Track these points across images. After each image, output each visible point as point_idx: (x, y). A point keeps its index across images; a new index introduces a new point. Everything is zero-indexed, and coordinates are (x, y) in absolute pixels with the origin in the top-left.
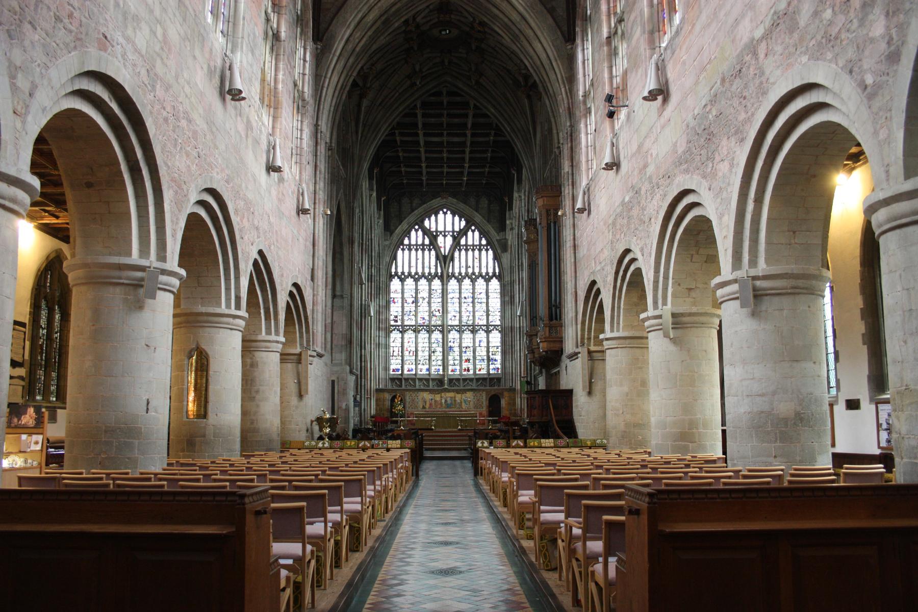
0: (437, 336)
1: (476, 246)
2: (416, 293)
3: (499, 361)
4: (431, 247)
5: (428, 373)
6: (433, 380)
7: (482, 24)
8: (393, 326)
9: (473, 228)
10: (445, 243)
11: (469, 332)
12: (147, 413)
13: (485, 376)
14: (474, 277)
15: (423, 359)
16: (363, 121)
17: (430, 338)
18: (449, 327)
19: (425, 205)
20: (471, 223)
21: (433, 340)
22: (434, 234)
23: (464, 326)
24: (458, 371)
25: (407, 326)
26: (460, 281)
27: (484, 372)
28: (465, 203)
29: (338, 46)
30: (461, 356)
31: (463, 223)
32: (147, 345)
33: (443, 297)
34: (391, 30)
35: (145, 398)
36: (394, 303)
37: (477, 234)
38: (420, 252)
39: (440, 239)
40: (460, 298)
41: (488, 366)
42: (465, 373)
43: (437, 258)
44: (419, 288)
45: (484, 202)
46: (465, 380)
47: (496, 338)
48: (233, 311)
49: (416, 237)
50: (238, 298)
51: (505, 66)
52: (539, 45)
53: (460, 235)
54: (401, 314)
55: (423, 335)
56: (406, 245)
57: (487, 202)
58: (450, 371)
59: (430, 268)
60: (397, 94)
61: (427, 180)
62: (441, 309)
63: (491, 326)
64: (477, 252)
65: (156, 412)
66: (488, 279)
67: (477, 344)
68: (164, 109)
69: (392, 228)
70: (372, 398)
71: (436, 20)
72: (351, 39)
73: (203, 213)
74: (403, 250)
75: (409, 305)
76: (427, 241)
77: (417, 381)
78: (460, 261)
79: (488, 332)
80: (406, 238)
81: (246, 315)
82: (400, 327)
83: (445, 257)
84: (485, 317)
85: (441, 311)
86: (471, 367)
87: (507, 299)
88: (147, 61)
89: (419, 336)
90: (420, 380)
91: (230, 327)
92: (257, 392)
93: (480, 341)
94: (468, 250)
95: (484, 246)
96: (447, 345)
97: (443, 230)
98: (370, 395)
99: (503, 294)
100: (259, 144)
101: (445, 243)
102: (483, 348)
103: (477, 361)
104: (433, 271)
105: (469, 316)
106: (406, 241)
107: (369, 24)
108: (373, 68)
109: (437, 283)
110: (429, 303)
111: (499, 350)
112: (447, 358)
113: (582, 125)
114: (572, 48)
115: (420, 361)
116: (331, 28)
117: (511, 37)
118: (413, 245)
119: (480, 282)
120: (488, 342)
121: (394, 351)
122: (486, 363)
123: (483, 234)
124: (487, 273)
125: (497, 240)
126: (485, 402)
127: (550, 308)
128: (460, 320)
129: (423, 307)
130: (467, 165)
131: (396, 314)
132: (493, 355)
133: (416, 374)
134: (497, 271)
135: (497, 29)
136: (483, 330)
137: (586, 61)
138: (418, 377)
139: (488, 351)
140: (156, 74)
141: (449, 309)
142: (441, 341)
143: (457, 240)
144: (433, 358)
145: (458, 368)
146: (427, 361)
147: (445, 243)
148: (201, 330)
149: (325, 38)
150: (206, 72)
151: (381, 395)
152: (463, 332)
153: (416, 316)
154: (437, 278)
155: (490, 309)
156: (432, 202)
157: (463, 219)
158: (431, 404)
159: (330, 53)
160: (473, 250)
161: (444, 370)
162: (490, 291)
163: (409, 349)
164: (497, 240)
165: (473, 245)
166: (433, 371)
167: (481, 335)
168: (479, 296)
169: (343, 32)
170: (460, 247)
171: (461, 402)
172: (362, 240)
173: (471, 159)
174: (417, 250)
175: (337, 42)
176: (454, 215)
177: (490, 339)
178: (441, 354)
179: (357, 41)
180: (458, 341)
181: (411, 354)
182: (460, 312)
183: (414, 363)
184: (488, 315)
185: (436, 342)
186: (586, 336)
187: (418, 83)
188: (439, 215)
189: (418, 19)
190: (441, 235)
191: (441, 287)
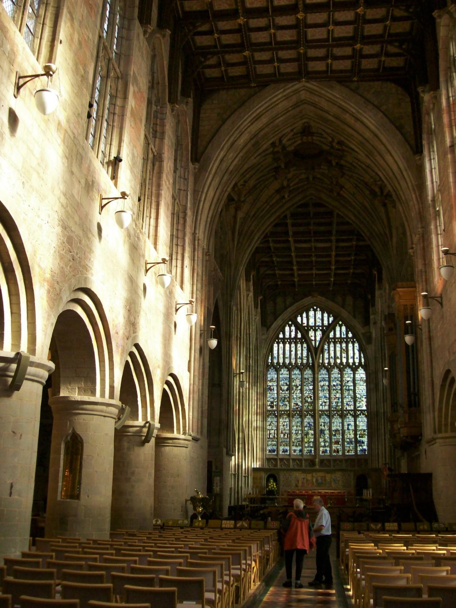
0: (308, 420)
1: (344, 338)
2: (290, 381)
3: (366, 443)
4: (303, 340)
5: (301, 453)
6: (306, 460)
7: (340, 143)
8: (269, 411)
9: (340, 323)
10: (315, 336)
11: (338, 417)
12: (10, 496)
13: (354, 457)
14: (342, 366)
15: (296, 441)
16: (239, 230)
17: (302, 422)
18: (320, 412)
20: (338, 319)
21: (305, 424)
22: (306, 328)
24: (328, 452)
25: (282, 411)
26: (329, 370)
27: (352, 453)
28: (333, 301)
29: (214, 166)
30: (330, 438)
31: (331, 319)
32: (14, 432)
33: (314, 385)
34: (260, 151)
35: (9, 482)
36: (271, 390)
37: (344, 328)
38: (293, 345)
39: (312, 333)
40: (329, 386)
41: (356, 448)
42: (335, 454)
43: (309, 350)
44: (293, 377)
45: (349, 300)
46: (335, 460)
47: (362, 423)
48: (107, 399)
49: (290, 331)
50: (112, 387)
51: (362, 178)
52: (390, 158)
53: (330, 329)
55: (296, 420)
56: (281, 339)
58: (321, 452)
59: (302, 358)
60: (268, 206)
61: (298, 281)
62: (312, 396)
63: (359, 411)
64: (344, 345)
65: (19, 495)
66: (354, 369)
67: (346, 427)
68: (39, 217)
70: (250, 476)
71: (299, 142)
72: (225, 159)
73: (79, 310)
74: (278, 343)
75: (284, 392)
76: (299, 336)
77: (291, 461)
78: (329, 353)
79: (355, 417)
80: (281, 333)
81: (119, 404)
83: (316, 349)
84: (352, 403)
85: (312, 398)
86: (339, 447)
87: (372, 386)
88: (23, 175)
90: (294, 460)
91: (103, 414)
92: (133, 473)
93: (348, 425)
94: (337, 342)
95: (350, 338)
96: (318, 428)
97: (313, 325)
98: (248, 474)
99: (368, 381)
100: (137, 249)
101: (316, 336)
102: (351, 431)
103: (346, 443)
104: (305, 361)
105: (338, 402)
106: (281, 336)
107: (240, 147)
108: (247, 184)
109: (308, 373)
110: (302, 391)
111: (366, 433)
112: (319, 441)
113: (432, 227)
114: (420, 159)
115: (294, 442)
116: (207, 151)
117: (367, 153)
118: (287, 339)
119: (348, 371)
120: (356, 425)
121: (270, 434)
124: (354, 363)
126: (353, 482)
127: (409, 395)
128: (329, 406)
129: (297, 394)
130: (333, 267)
131: (272, 400)
132: (360, 437)
133: (290, 455)
134: (363, 360)
135: (353, 147)
136: (351, 415)
137: (433, 170)
138: (292, 457)
139: (355, 435)
140: (31, 186)
141: (320, 395)
142: (312, 424)
143: (326, 334)
144: (306, 440)
145: (328, 449)
146: (300, 443)
147: (315, 336)
148: (76, 418)
149: (202, 159)
150: (84, 186)
151: (258, 474)
152: (333, 417)
153: (289, 402)
154: (308, 368)
155: (358, 396)
156: (304, 300)
157: (331, 315)
158: (303, 483)
159: (207, 171)
160: (341, 343)
161: (315, 451)
163: (284, 432)
164: (362, 334)
165: (341, 338)
167: (350, 420)
169: (217, 153)
170: (329, 340)
171: (331, 481)
172: (240, 335)
173: (337, 262)
174: (290, 344)
175: (213, 162)
177: (357, 423)
178: (313, 437)
179: (230, 161)
181: (286, 437)
182: (330, 398)
183: (288, 445)
184: (355, 402)
185: (308, 425)
186: (443, 422)
187: (286, 196)
188: (310, 312)
189: (284, 141)
191: (312, 377)
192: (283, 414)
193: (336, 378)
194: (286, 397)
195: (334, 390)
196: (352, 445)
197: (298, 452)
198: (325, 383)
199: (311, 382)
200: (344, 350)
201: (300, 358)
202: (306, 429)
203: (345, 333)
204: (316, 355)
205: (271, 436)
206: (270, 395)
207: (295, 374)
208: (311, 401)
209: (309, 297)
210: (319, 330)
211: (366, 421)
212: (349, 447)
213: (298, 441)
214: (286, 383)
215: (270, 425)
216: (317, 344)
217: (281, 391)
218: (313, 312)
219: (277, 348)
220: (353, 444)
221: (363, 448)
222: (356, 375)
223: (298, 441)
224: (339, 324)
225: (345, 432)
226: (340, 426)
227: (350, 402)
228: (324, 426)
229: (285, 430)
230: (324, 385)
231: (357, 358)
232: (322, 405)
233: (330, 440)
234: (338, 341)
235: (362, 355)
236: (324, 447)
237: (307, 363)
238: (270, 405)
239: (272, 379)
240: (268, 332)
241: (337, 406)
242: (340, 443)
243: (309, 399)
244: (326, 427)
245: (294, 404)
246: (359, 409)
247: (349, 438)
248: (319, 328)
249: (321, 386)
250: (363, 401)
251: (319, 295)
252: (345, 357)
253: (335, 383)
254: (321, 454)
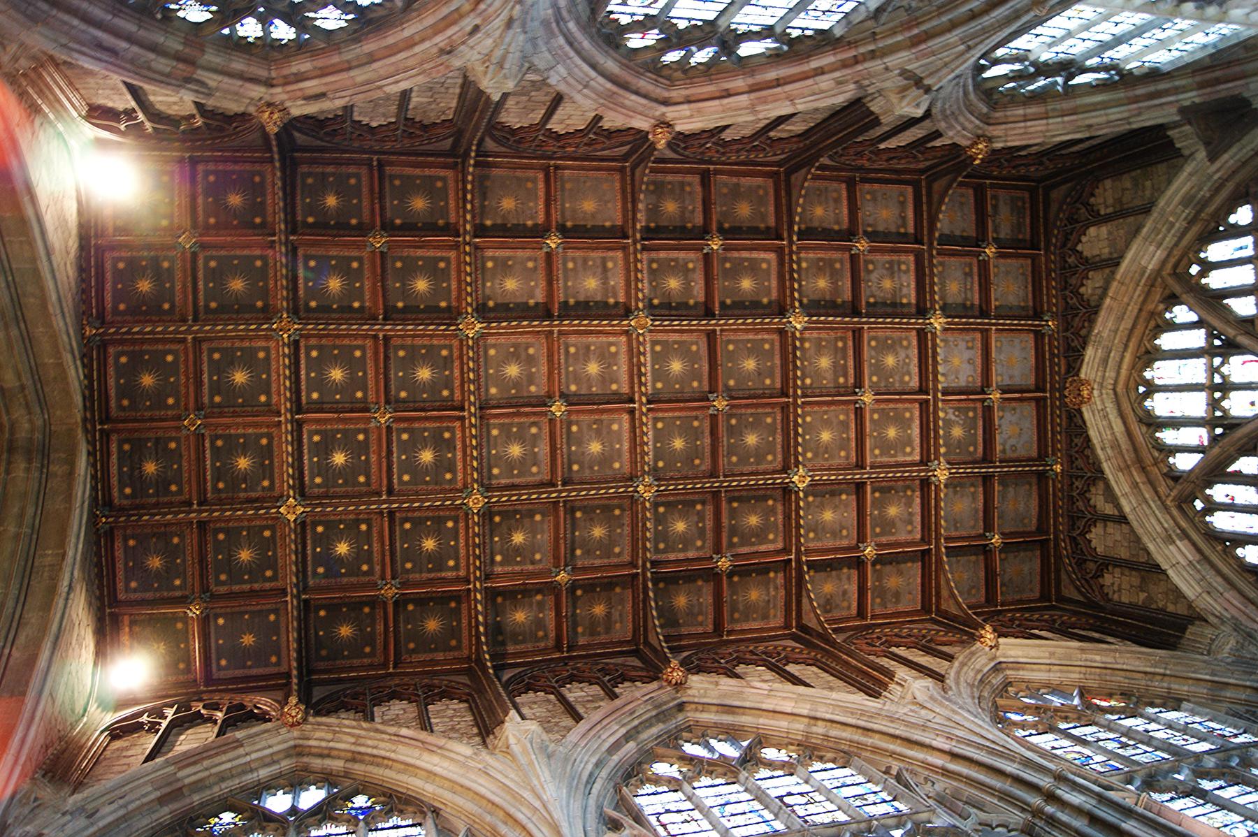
9: (1194, 269)
19: (1106, 467)
28: (1092, 311)
31: (1182, 314)
37: (1216, 251)
45: (1095, 241)
57: (1092, 231)
69: (1181, 610)
80: (1240, 552)
123: (1219, 230)
125: (1212, 158)
157: (1168, 315)
164: (1212, 158)
176: (1153, 355)
188: (1158, 412)
190: (1225, 404)
209: (1087, 415)
210: (1225, 370)
218: (1157, 396)
224: (1203, 274)
240: (1211, 619)
251: (1079, 370)
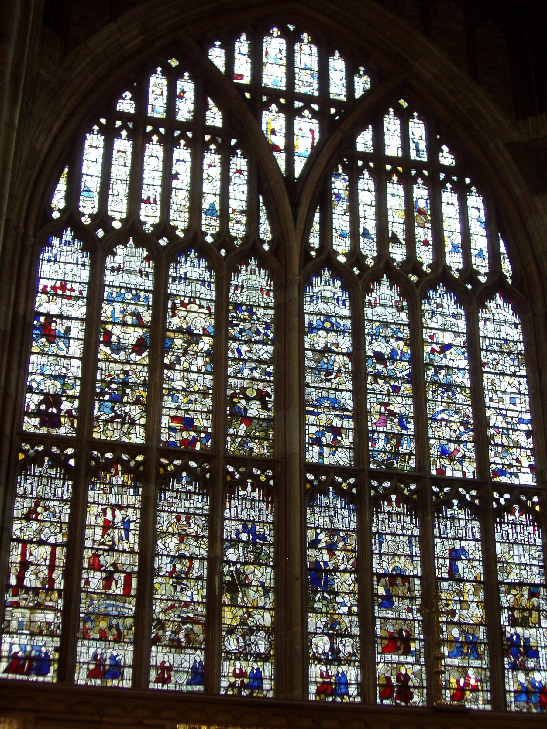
1: (419, 166)
4: (233, 142)
8: (33, 439)
10: (290, 134)
14: (414, 278)
18: (310, 477)
22: (248, 95)
23: (380, 476)
24: (353, 690)
36: (52, 337)
44: (173, 288)
54: (76, 391)
56: (125, 117)
63: (502, 488)
75: (122, 356)
80: (128, 94)
82: (70, 451)
89: (163, 505)
94: (388, 176)
96: (304, 555)
105: (399, 437)
115: (161, 624)
118: (156, 122)
121: (25, 565)
122: (484, 663)
132: (514, 623)
136: (463, 504)
141: (311, 394)
142: (269, 533)
146: (197, 628)
147: (290, 134)
154: (253, 262)
155: (495, 420)
162: (484, 344)
163: (106, 560)
166: (224, 683)
168: (438, 359)
178: (269, 601)
180: (353, 542)
181: (117, 589)
183: (130, 636)
185: (244, 537)
188: (267, 39)
192: (108, 466)
193: (386, 325)
194: (132, 379)
195: (377, 376)
196: (477, 663)
197: (184, 678)
198: (332, 337)
199: (267, 327)
200: (421, 212)
201: (212, 210)
202: (232, 554)
203: (423, 145)
204: (295, 206)
205: (30, 580)
206: (44, 359)
207: (185, 278)
208: (264, 415)
210: (306, 112)
211: (539, 541)
212: (463, 670)
213: (185, 621)
214: (137, 315)
215: (27, 518)
216: (299, 167)
217: (107, 350)
219: (101, 151)
220: (479, 657)
221: (532, 683)
222: (481, 324)
223: (185, 621)
225: (438, 590)
226: (411, 556)
227: (457, 441)
228: (331, 548)
229: (112, 549)
230: (326, 350)
231: (480, 254)
232: (317, 441)
233: (361, 626)
234: (394, 171)
235: (503, 249)
236: (328, 662)
237: (245, 239)
238: (37, 413)
239: (63, 287)
241: (396, 454)
242: (413, 646)
243: (255, 405)
244: (340, 555)
245: (174, 419)
246: (504, 479)
247: (459, 624)
248: (307, 106)
249: (314, 350)
250: (518, 446)
252: (426, 243)
253: (381, 347)
254: (312, 697)
